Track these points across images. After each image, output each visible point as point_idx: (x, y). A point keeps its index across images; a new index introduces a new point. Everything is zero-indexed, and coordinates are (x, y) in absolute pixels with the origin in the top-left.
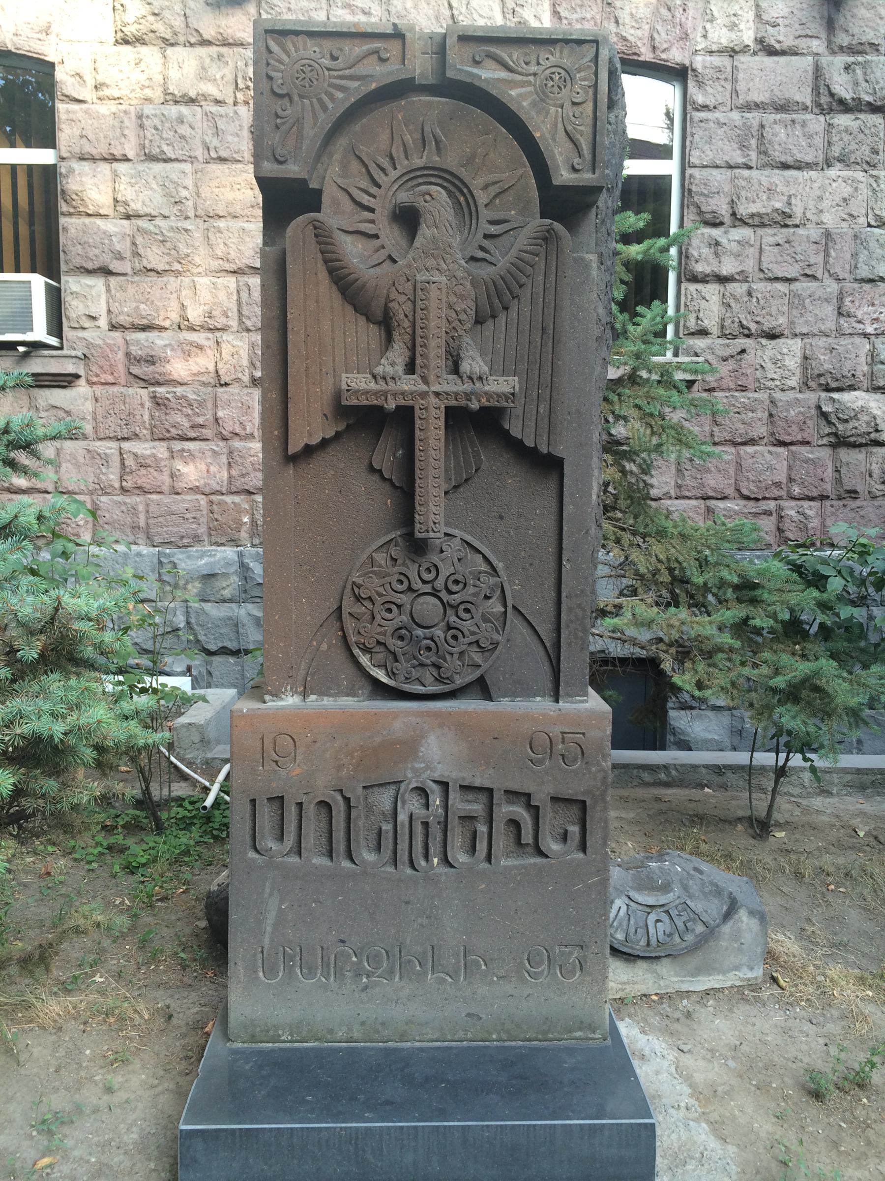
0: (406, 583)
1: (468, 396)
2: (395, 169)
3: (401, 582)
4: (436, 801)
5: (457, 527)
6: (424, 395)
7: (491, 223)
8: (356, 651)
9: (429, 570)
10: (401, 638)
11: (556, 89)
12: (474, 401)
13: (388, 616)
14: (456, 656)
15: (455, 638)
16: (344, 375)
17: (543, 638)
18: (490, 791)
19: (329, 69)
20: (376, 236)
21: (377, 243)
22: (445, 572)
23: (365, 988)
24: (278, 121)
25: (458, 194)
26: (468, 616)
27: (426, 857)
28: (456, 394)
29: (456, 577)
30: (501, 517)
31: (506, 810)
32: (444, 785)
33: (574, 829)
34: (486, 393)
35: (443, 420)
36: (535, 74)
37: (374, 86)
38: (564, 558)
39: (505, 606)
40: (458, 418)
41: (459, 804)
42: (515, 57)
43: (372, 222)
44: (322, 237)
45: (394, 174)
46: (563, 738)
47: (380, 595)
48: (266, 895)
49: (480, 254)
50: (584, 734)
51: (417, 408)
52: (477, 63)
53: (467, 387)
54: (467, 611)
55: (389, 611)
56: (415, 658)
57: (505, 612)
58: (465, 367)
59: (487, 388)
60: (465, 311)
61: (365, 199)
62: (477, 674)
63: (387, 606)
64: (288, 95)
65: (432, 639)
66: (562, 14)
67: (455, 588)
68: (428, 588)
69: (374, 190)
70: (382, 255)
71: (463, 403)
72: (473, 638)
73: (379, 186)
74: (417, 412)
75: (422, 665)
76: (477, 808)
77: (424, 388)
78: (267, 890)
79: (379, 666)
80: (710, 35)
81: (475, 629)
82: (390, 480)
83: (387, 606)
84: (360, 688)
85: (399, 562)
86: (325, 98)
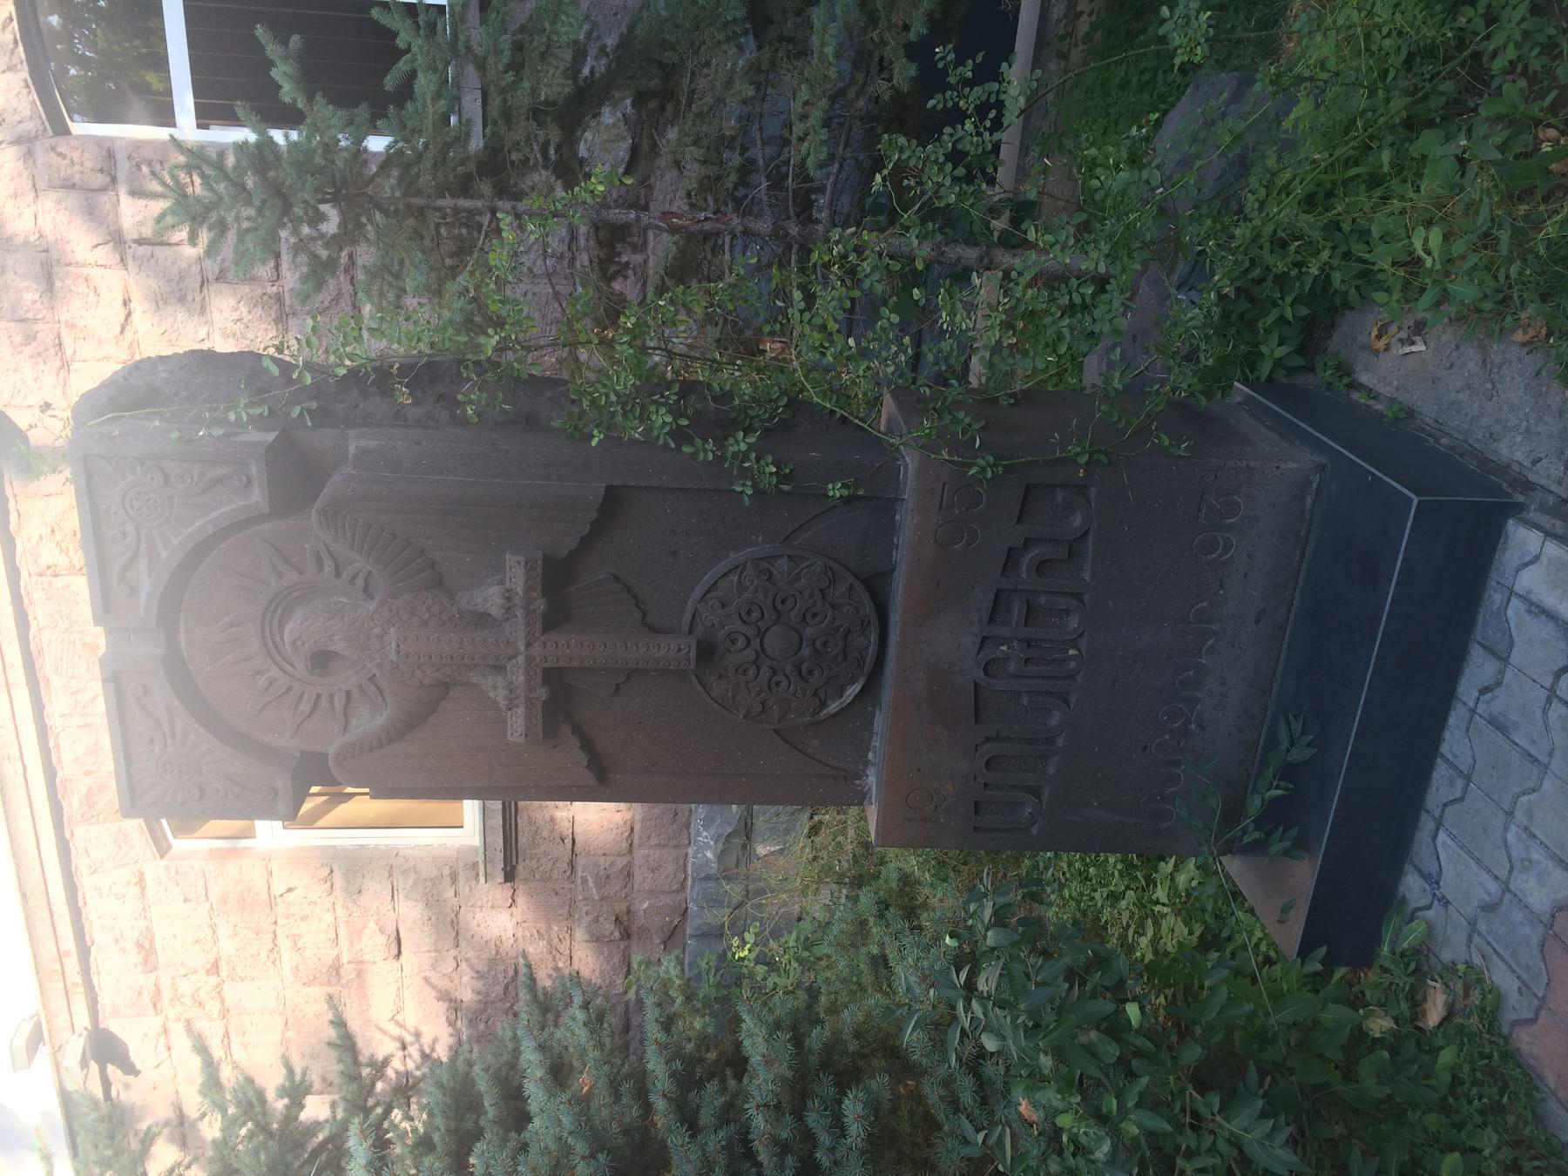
1: (529, 612)
6: (530, 660)
7: (320, 567)
9: (733, 642)
10: (810, 672)
13: (784, 684)
20: (348, 693)
21: (356, 694)
22: (736, 625)
23: (1202, 727)
26: (789, 603)
28: (528, 625)
30: (675, 553)
36: (137, 528)
37: (177, 704)
43: (332, 697)
47: (761, 692)
49: (360, 582)
52: (134, 591)
53: (519, 612)
54: (783, 602)
55: (778, 684)
67: (756, 614)
68: (756, 643)
73: (291, 687)
75: (844, 651)
77: (521, 659)
79: (842, 690)
81: (806, 594)
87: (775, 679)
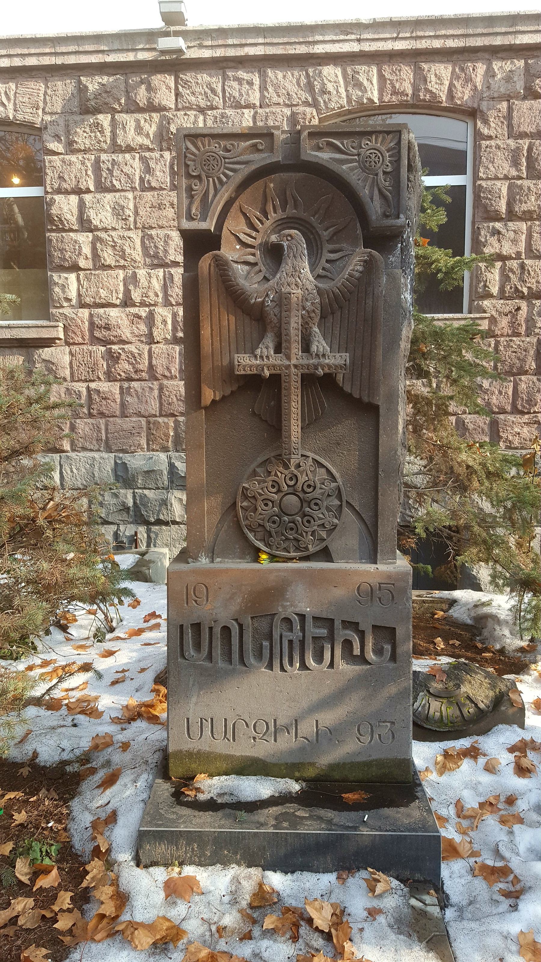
0: (277, 487)
1: (316, 367)
2: (268, 219)
3: (273, 486)
4: (297, 626)
5: (310, 451)
6: (288, 367)
8: (246, 531)
9: (291, 479)
10: (274, 522)
11: (373, 163)
12: (320, 370)
13: (266, 508)
14: (310, 533)
15: (309, 522)
16: (236, 355)
17: (367, 521)
18: (332, 621)
19: (224, 158)
24: (193, 193)
25: (309, 234)
26: (316, 508)
27: (291, 664)
28: (308, 365)
29: (309, 482)
31: (342, 634)
32: (302, 617)
33: (388, 647)
34: (328, 365)
35: (300, 382)
38: (380, 470)
39: (341, 501)
40: (309, 380)
41: (312, 630)
42: (345, 142)
43: (254, 255)
44: (221, 265)
45: (268, 223)
46: (380, 586)
47: (260, 495)
48: (190, 685)
50: (393, 584)
51: (283, 375)
54: (316, 504)
55: (266, 505)
56: (283, 535)
57: (341, 506)
58: (314, 348)
59: (327, 361)
60: (314, 311)
61: (249, 241)
62: (324, 545)
63: (265, 502)
64: (199, 177)
65: (293, 522)
66: (387, 76)
68: (291, 490)
69: (254, 234)
70: (260, 277)
71: (312, 371)
72: (320, 522)
73: (258, 232)
74: (283, 378)
75: (287, 539)
76: (323, 632)
77: (288, 363)
78: (191, 683)
79: (260, 540)
80: (492, 86)
81: (321, 516)
82: (266, 421)
83: (265, 502)
84: (249, 554)
85: (273, 473)
86: (222, 176)
87: (270, 504)
